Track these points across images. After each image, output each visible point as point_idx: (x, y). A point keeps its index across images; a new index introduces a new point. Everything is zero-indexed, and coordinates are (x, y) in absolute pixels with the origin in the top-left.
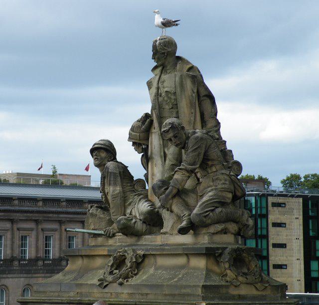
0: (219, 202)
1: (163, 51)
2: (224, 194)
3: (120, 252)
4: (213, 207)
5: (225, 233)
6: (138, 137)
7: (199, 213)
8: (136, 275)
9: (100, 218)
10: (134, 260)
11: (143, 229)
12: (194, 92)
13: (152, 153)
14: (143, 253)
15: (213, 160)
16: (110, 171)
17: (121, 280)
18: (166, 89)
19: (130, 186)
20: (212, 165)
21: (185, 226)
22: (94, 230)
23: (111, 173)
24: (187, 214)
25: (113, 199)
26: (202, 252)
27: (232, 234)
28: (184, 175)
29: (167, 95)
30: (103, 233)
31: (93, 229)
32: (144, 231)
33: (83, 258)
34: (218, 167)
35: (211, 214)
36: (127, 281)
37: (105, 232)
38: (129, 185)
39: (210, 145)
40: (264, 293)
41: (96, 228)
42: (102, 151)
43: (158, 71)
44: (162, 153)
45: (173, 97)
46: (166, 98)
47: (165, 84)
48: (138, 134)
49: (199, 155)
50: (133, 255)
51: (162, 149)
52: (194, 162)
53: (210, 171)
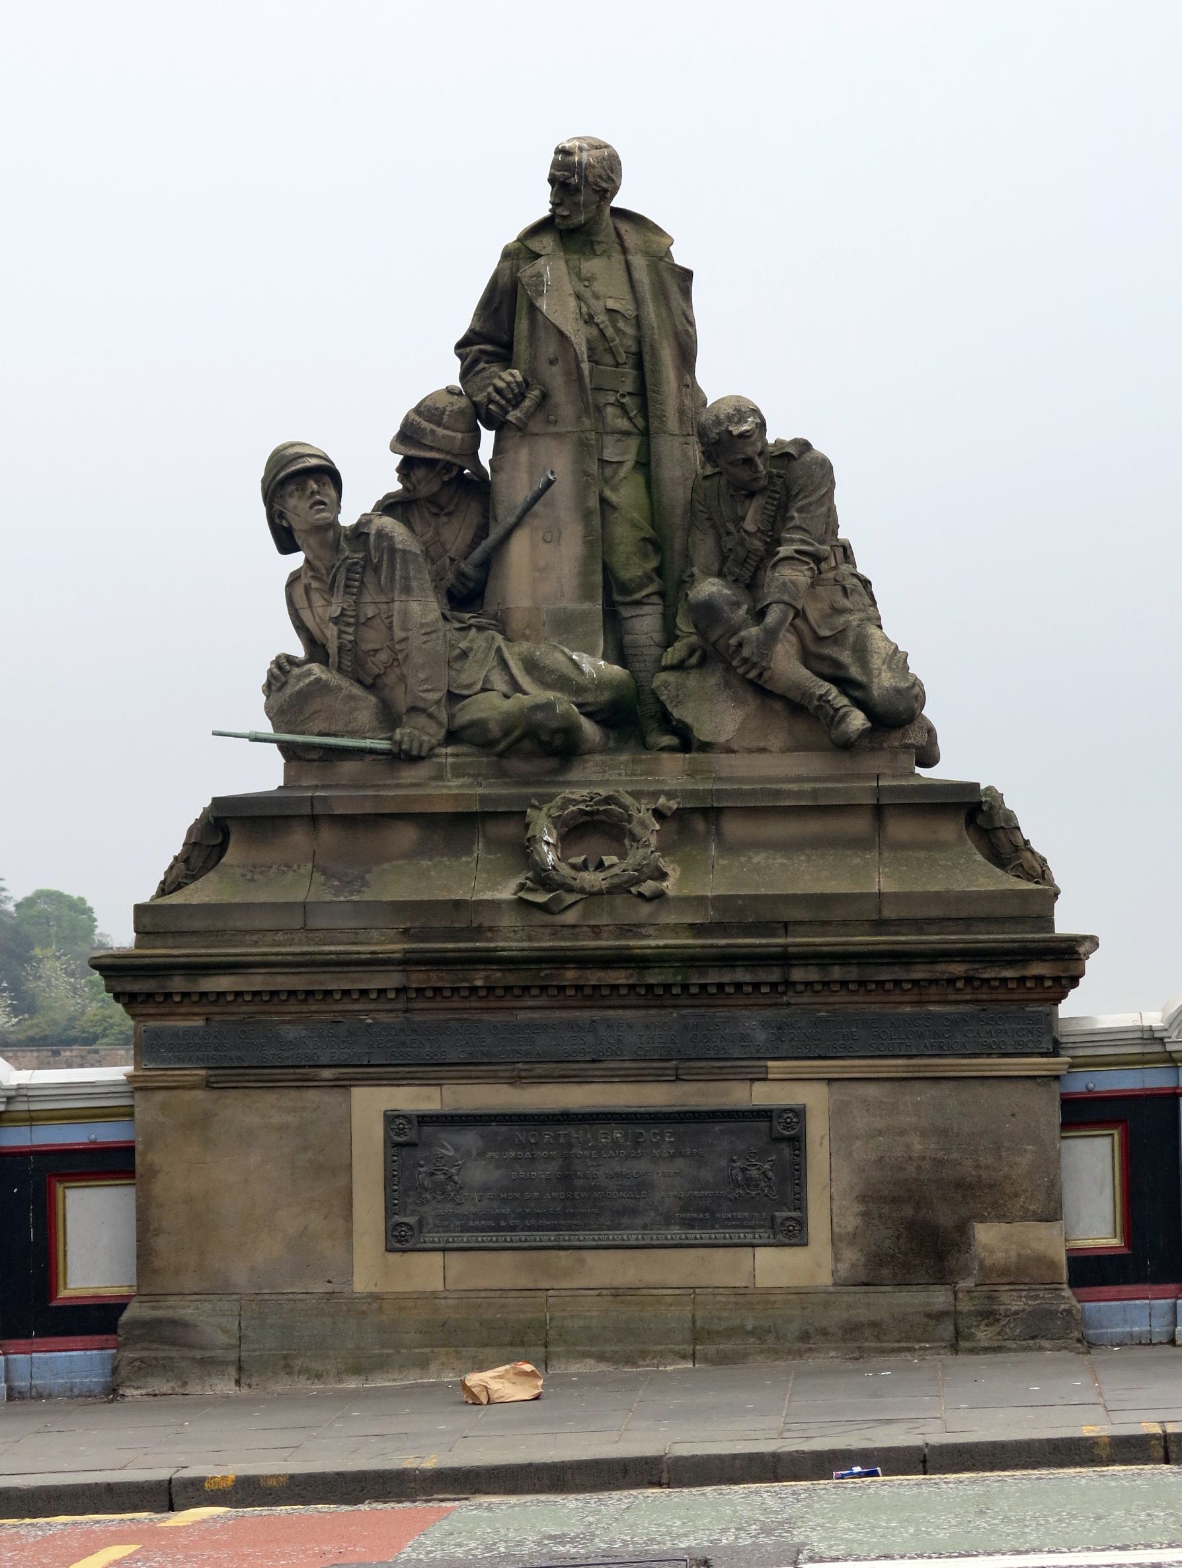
1: (604, 185)
3: (575, 802)
9: (352, 697)
14: (674, 805)
25: (425, 638)
31: (320, 734)
48: (459, 436)
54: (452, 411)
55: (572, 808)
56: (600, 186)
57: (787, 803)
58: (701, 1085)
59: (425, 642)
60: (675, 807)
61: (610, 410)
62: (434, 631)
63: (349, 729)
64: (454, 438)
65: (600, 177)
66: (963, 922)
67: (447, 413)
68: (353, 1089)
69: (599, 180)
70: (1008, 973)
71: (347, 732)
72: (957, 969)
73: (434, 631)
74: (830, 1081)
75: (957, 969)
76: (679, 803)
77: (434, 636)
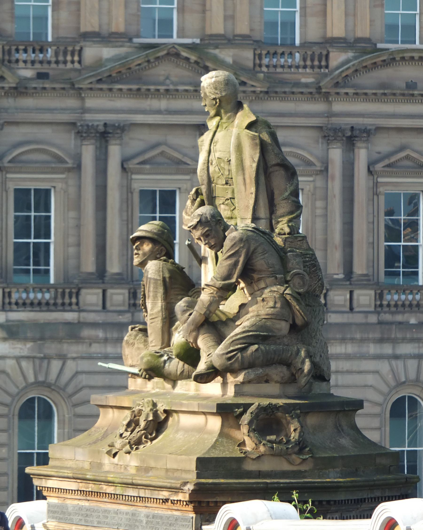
5: (267, 381)
8: (152, 440)
11: (177, 370)
12: (254, 161)
15: (260, 271)
16: (149, 276)
20: (259, 280)
21: (203, 372)
23: (150, 278)
27: (277, 382)
32: (179, 373)
35: (239, 354)
39: (255, 249)
41: (134, 363)
42: (147, 241)
49: (236, 264)
53: (256, 288)
59: (152, 323)
61: (222, 206)
72: (165, 494)
75: (165, 494)
77: (156, 319)
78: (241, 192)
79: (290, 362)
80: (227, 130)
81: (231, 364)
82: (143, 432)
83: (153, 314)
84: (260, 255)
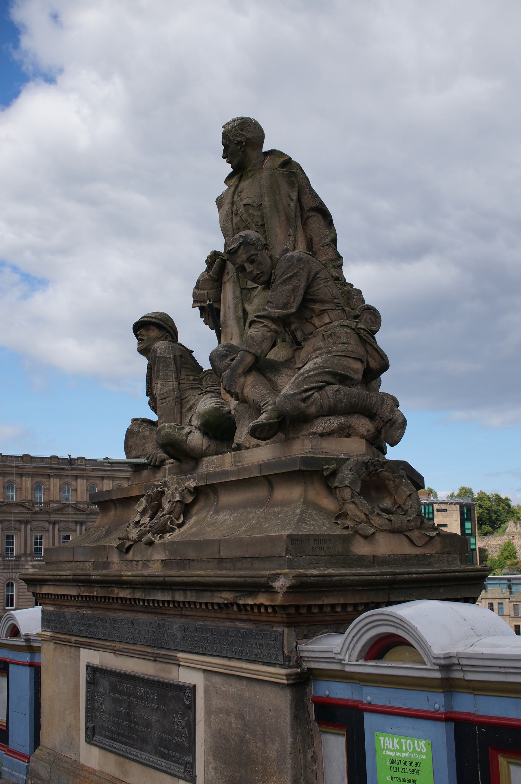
0: (334, 374)
1: (239, 139)
2: (346, 362)
4: (321, 382)
5: (348, 436)
6: (206, 295)
7: (291, 392)
8: (180, 526)
9: (144, 437)
10: (178, 498)
12: (292, 200)
13: (225, 317)
14: (193, 485)
15: (323, 302)
16: (158, 355)
17: (150, 535)
18: (245, 201)
19: (194, 380)
20: (323, 312)
21: (264, 421)
22: (136, 458)
23: (159, 357)
24: (271, 401)
26: (294, 469)
27: (362, 437)
28: (266, 329)
29: (247, 211)
30: (146, 461)
32: (204, 448)
33: (114, 503)
34: (333, 315)
35: (316, 395)
36: (161, 538)
37: (147, 459)
38: (192, 378)
39: (317, 273)
40: (427, 551)
43: (235, 180)
44: (240, 313)
45: (256, 213)
46: (245, 216)
47: (243, 195)
48: (206, 292)
49: (294, 290)
50: (176, 489)
51: (240, 305)
52: (287, 304)
54: (203, 280)
55: (155, 489)
56: (237, 141)
57: (229, 480)
58: (163, 665)
59: (162, 404)
60: (195, 485)
62: (167, 397)
63: (143, 453)
64: (204, 294)
65: (235, 136)
66: (249, 560)
67: (201, 281)
68: (82, 649)
69: (235, 138)
70: (250, 602)
71: (143, 455)
72: (227, 596)
73: (167, 397)
74: (205, 671)
75: (227, 596)
76: (196, 483)
77: (167, 400)
78: (276, 236)
79: (375, 412)
80: (254, 177)
81: (307, 407)
82: (167, 516)
83: (163, 394)
84: (323, 281)
